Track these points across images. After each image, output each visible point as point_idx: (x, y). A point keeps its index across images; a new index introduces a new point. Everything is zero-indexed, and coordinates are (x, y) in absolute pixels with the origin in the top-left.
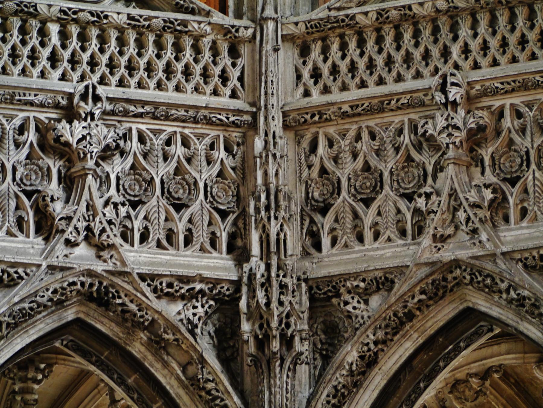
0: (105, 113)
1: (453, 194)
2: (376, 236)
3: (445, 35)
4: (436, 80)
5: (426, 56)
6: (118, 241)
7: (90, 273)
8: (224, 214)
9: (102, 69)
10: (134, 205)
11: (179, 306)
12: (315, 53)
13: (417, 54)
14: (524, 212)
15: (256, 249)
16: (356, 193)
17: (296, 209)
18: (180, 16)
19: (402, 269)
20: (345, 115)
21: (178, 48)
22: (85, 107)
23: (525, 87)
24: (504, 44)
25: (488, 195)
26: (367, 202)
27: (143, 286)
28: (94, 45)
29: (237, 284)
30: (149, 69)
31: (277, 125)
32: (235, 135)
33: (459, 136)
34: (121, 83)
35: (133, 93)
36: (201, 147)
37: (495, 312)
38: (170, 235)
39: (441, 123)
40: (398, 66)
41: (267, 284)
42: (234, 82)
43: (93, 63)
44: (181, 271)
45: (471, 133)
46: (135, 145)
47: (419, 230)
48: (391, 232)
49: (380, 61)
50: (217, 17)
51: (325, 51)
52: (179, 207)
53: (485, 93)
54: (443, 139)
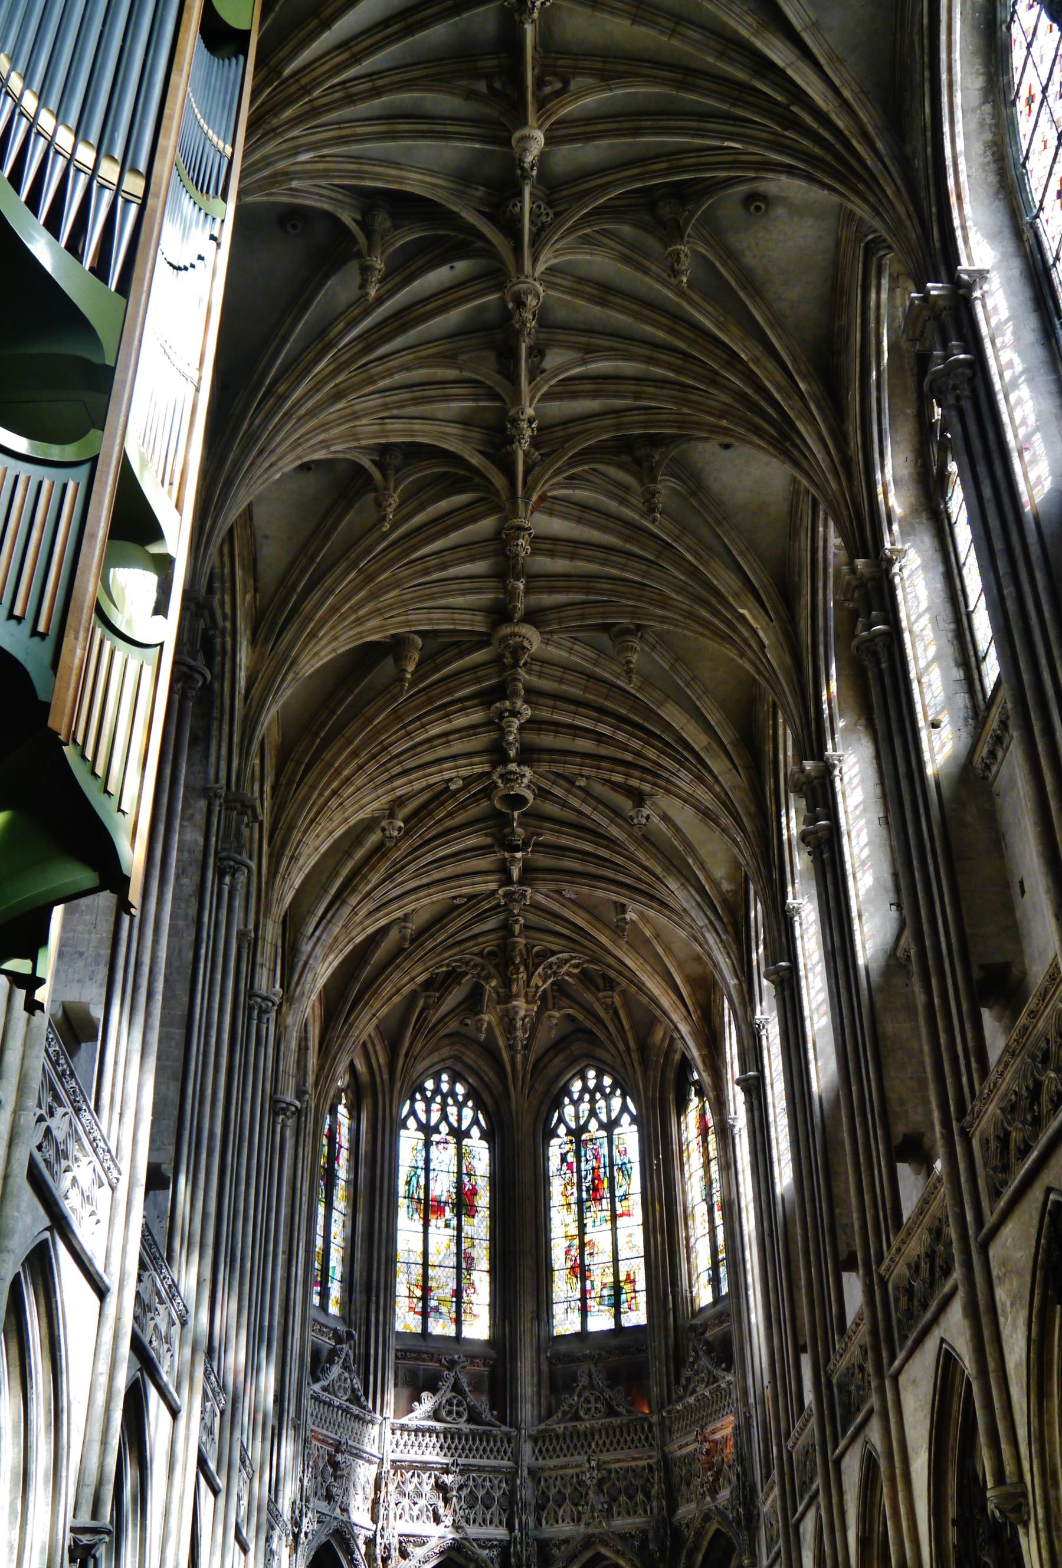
0: (460, 1470)
1: (592, 1506)
2: (563, 1521)
3: (589, 1439)
4: (586, 1457)
5: (582, 1446)
6: (464, 1524)
7: (453, 1539)
8: (504, 1511)
9: (460, 1451)
10: (471, 1508)
11: (487, 1551)
12: (540, 1443)
13: (579, 1445)
14: (619, 1514)
15: (517, 1527)
16: (556, 1502)
17: (532, 1508)
18: (489, 1428)
19: (573, 1538)
20: (551, 1469)
21: (488, 1441)
22: (454, 1469)
23: (619, 1461)
24: (611, 1442)
25: (606, 1506)
26: (560, 1506)
27: (474, 1544)
28: (456, 1441)
29: (509, 1542)
30: (477, 1450)
31: (525, 1473)
32: (509, 1477)
33: (595, 1481)
34: (467, 1457)
35: (471, 1461)
36: (496, 1482)
37: (608, 1554)
38: (484, 1521)
39: (588, 1475)
40: (572, 1450)
41: (521, 1543)
42: (509, 1454)
43: (456, 1449)
44: (488, 1537)
45: (599, 1480)
46: (471, 1483)
47: (579, 1519)
48: (568, 1520)
49: (565, 1447)
50: (504, 1428)
51: (544, 1442)
52: (488, 1508)
53: (605, 1463)
54: (589, 1482)
